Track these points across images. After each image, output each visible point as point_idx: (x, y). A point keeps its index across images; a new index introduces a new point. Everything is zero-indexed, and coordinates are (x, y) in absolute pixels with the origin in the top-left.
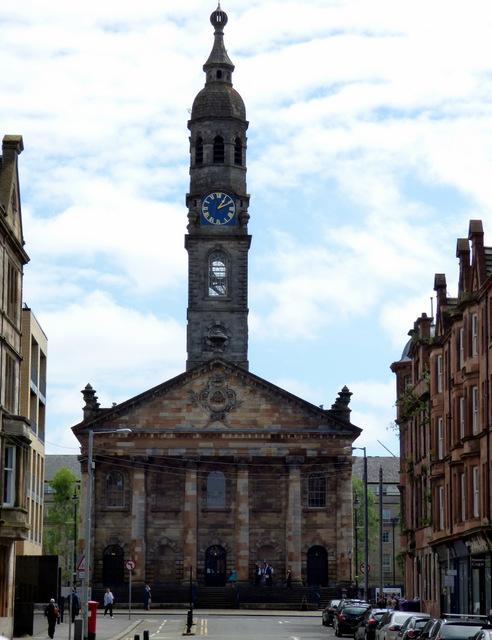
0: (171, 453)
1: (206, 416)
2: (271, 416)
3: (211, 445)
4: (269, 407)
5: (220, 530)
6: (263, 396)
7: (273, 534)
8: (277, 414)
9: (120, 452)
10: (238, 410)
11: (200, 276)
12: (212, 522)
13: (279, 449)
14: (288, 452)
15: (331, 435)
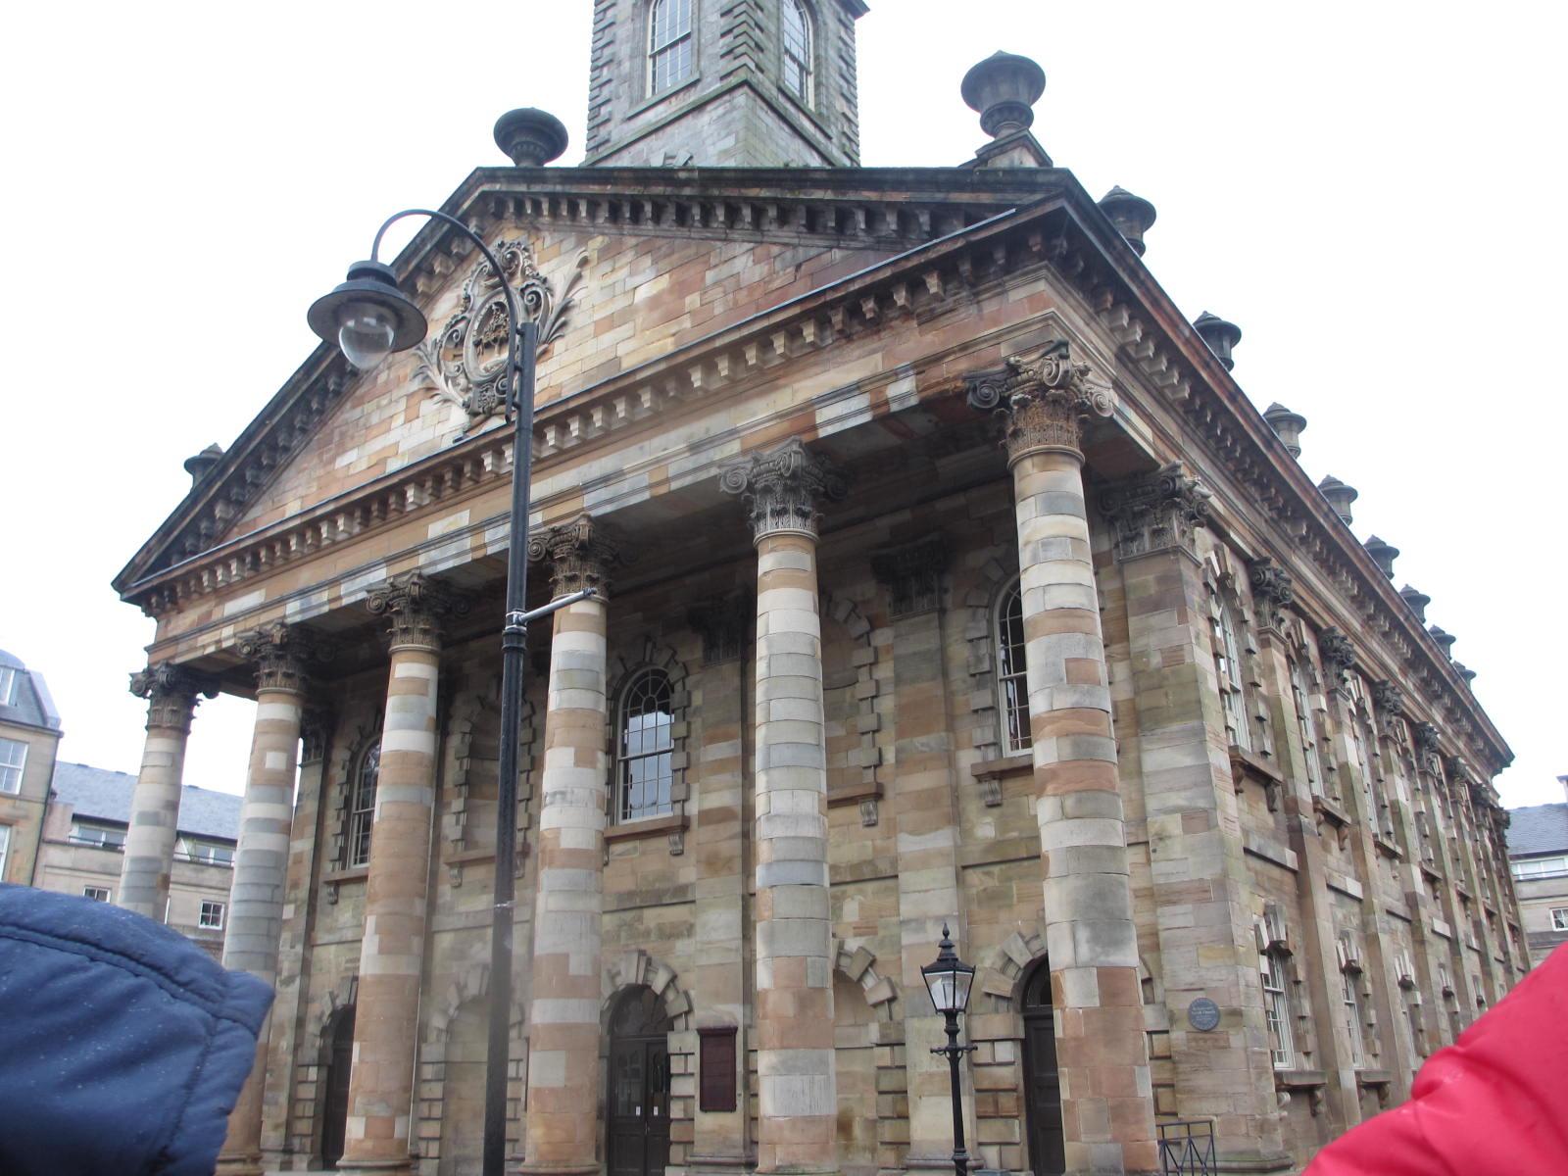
0: (352, 592)
1: (458, 418)
2: (672, 316)
3: (462, 518)
4: (664, 282)
5: (652, 917)
6: (644, 250)
7: (851, 910)
8: (693, 300)
9: (227, 636)
10: (558, 346)
11: (619, 64)
12: (627, 884)
13: (695, 448)
14: (734, 447)
15: (913, 280)
